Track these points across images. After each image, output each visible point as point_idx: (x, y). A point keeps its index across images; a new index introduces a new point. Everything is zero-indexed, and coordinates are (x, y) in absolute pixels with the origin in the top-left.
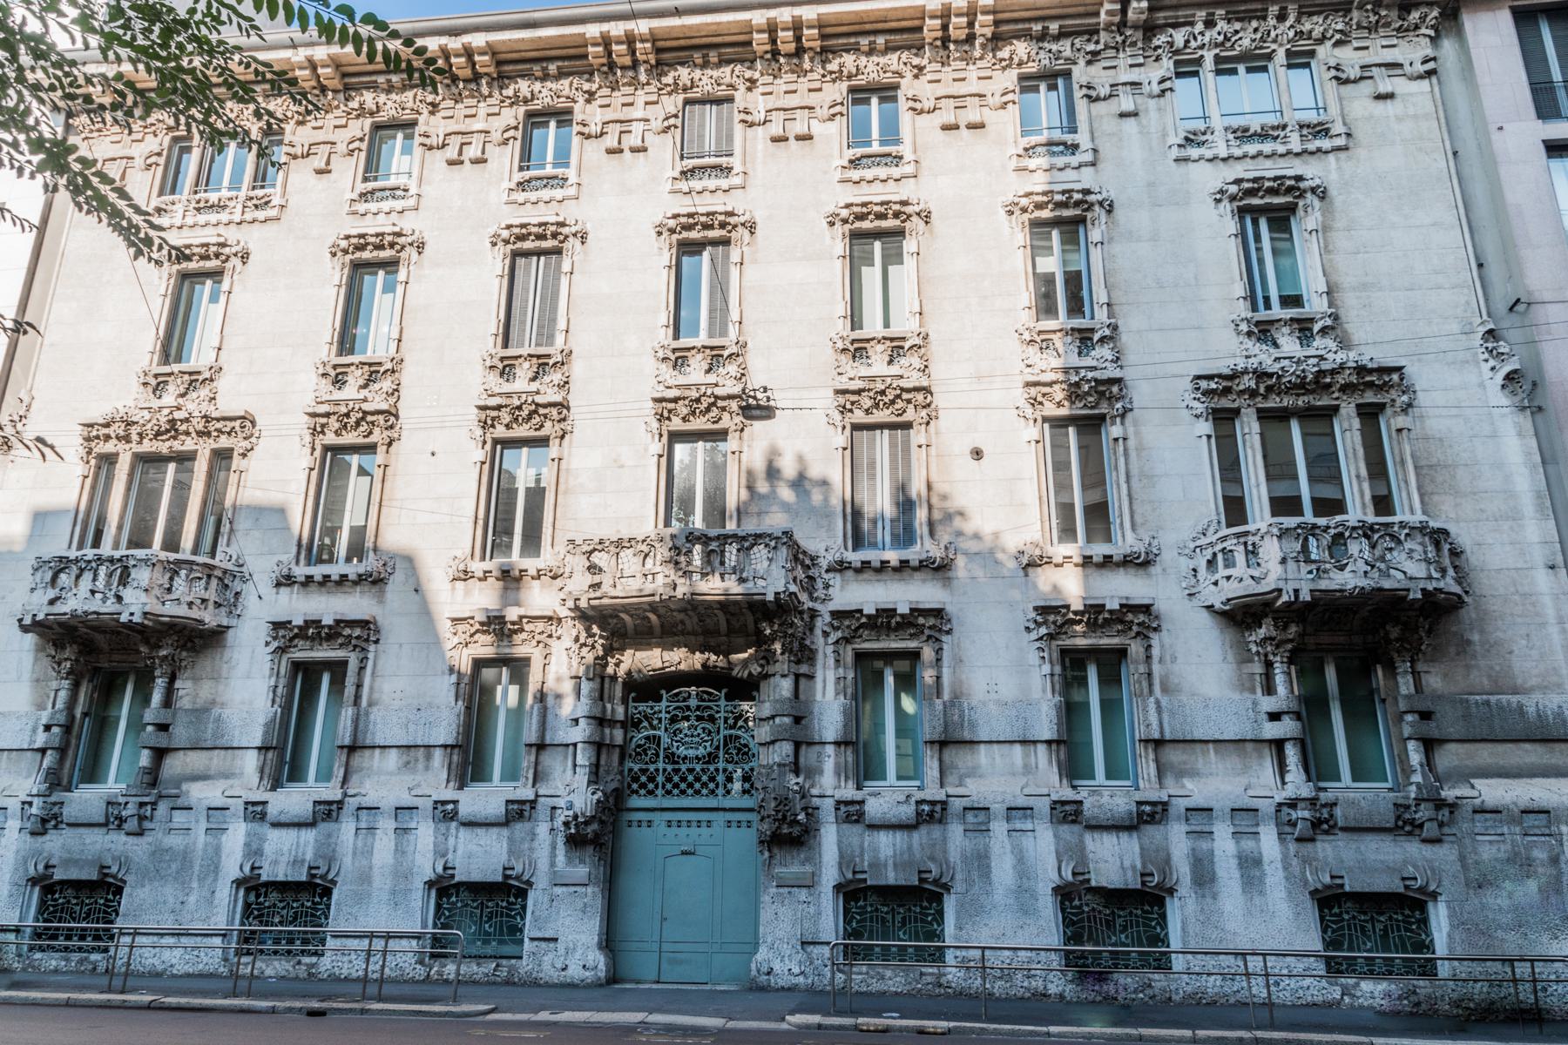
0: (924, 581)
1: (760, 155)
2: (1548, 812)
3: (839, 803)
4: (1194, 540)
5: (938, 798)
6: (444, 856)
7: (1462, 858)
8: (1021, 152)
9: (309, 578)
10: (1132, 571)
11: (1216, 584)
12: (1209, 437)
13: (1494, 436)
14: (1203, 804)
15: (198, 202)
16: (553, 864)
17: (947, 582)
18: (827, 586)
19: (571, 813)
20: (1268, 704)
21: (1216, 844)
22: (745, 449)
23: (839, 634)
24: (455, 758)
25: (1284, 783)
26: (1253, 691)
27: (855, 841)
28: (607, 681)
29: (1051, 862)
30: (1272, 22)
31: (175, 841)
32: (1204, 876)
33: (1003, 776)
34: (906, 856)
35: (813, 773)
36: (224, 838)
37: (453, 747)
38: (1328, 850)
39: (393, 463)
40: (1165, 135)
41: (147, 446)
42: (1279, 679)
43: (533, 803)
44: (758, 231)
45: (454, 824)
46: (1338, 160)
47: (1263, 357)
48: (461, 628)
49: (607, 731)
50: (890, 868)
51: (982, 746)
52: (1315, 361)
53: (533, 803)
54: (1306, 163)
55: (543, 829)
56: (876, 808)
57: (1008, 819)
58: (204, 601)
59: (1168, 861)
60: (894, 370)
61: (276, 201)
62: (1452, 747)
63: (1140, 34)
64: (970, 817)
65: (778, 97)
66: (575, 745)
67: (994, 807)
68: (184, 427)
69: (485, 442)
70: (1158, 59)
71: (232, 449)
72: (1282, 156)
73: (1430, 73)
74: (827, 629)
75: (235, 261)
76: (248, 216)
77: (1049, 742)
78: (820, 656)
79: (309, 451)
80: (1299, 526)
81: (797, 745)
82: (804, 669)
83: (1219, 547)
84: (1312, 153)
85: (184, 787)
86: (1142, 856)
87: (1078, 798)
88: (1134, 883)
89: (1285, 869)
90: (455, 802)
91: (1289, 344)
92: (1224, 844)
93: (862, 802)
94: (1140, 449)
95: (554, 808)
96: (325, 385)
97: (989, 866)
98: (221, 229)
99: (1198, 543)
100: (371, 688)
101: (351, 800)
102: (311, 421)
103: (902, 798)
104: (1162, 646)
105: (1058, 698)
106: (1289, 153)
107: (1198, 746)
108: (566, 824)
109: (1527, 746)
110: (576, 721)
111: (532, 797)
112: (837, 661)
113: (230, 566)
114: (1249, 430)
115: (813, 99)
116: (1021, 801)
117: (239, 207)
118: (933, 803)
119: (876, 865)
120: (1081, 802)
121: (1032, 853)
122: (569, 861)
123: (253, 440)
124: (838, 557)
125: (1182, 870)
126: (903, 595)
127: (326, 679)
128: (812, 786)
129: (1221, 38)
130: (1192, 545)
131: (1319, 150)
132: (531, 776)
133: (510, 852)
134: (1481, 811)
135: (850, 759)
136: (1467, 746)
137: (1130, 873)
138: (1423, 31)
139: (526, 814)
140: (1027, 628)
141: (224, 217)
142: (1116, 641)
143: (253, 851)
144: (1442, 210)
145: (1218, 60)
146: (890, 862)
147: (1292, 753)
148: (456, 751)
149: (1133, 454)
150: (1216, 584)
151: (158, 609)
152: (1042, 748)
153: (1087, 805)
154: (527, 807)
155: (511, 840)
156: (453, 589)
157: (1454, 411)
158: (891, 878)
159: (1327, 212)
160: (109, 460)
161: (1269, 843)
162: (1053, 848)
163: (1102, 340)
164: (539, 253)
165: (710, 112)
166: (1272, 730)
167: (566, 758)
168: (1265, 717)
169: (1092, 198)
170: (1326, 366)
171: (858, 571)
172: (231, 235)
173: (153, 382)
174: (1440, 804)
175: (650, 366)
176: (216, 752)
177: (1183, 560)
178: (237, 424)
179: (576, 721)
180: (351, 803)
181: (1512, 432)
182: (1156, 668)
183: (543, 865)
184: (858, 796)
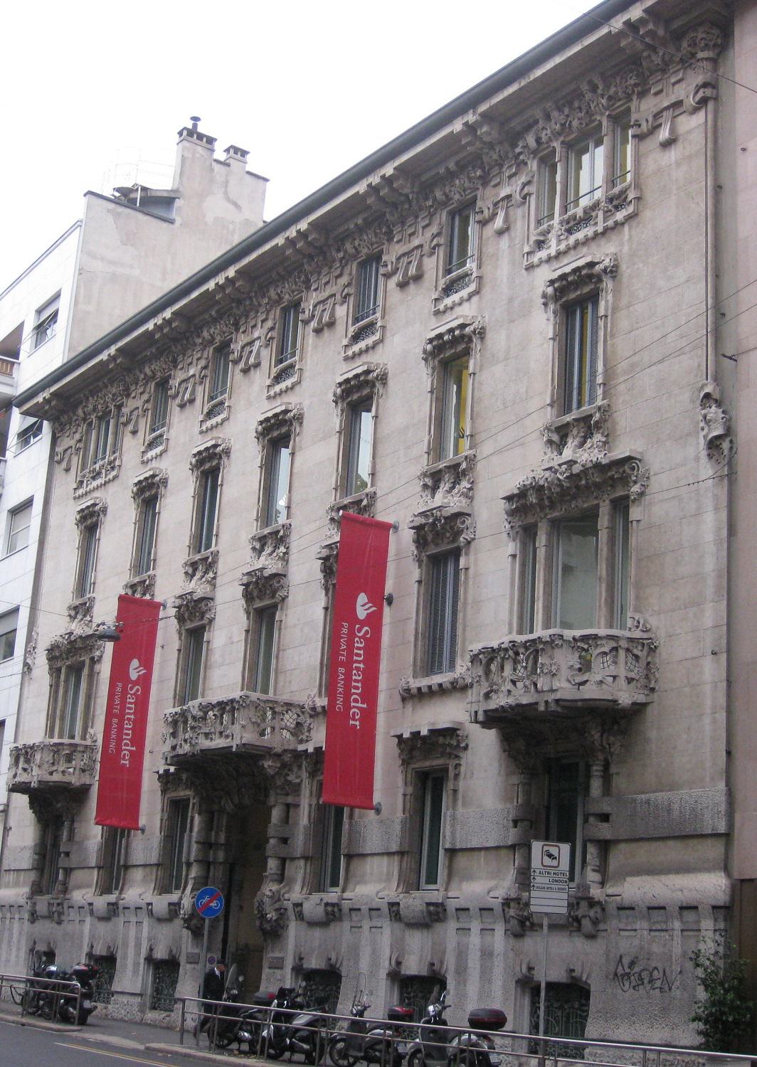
1: (310, 349)
2: (664, 908)
7: (607, 954)
10: (458, 695)
12: (514, 556)
13: (698, 514)
18: (309, 731)
22: (284, 618)
24: (159, 872)
29: (387, 952)
30: (588, 96)
35: (292, 881)
38: (534, 945)
40: (523, 245)
51: (369, 859)
57: (371, 919)
59: (444, 952)
62: (622, 846)
63: (507, 147)
64: (353, 914)
67: (363, 907)
73: (703, 102)
81: (283, 861)
82: (290, 800)
84: (613, 229)
88: (424, 972)
93: (301, 905)
103: (318, 901)
104: (467, 763)
106: (596, 235)
107: (477, 853)
109: (671, 843)
118: (333, 905)
120: (398, 904)
122: (192, 948)
128: (288, 892)
129: (558, 127)
131: (616, 224)
134: (621, 908)
136: (633, 845)
138: (701, 55)
142: (440, 762)
144: (694, 265)
145: (568, 146)
149: (471, 582)
153: (401, 906)
157: (673, 493)
160: (59, 670)
161: (499, 940)
169: (468, 330)
170: (576, 469)
174: (592, 903)
176: (86, 870)
181: (710, 508)
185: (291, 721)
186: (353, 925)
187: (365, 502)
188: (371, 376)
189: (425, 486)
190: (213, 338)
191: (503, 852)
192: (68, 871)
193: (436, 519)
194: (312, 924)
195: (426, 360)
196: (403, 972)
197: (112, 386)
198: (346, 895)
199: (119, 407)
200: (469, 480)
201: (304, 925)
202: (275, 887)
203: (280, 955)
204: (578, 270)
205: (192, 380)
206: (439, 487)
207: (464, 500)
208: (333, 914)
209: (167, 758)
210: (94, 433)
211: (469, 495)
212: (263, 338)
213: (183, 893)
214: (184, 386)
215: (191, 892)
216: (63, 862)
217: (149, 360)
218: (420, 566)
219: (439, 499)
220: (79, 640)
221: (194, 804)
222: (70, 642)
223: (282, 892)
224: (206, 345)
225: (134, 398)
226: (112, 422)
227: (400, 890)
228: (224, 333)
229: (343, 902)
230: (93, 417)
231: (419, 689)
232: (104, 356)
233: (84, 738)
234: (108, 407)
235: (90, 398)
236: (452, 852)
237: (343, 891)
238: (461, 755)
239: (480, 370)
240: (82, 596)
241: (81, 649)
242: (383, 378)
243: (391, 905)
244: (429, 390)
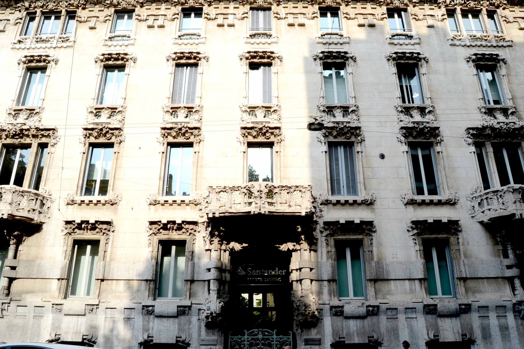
0: (363, 209)
3: (332, 308)
4: (472, 194)
5: (376, 304)
6: (148, 331)
8: (391, 37)
9: (83, 202)
11: (483, 212)
14: (486, 305)
15: (37, 39)
16: (200, 335)
17: (373, 210)
18: (321, 211)
19: (209, 312)
20: (507, 262)
21: (490, 321)
22: (282, 151)
23: (328, 232)
25: (514, 295)
26: (499, 257)
27: (339, 324)
28: (222, 251)
29: (425, 332)
31: (19, 321)
32: (486, 335)
33: (402, 294)
36: (42, 320)
37: (150, 281)
39: (121, 151)
41: (9, 141)
42: (510, 252)
43: (190, 307)
44: (284, 60)
45: (152, 316)
46: (509, 50)
47: (490, 121)
48: (154, 226)
49: (223, 274)
52: (513, 124)
53: (190, 307)
54: (498, 50)
55: (194, 319)
56: (348, 309)
57: (405, 313)
58: (34, 210)
59: (472, 329)
60: (346, 119)
61: (72, 39)
64: (389, 312)
65: (290, 9)
66: (209, 281)
67: (399, 308)
68: (27, 133)
69: (164, 144)
70: (440, 8)
71: (48, 144)
72: (489, 47)
74: (322, 230)
75: (52, 63)
76: (59, 45)
77: (420, 280)
78: (319, 242)
79: (83, 145)
80: (520, 188)
83: (485, 197)
84: (500, 47)
85: (23, 296)
86: (461, 327)
87: (435, 303)
88: (459, 339)
89: (518, 330)
90: (153, 306)
91: (501, 118)
92: (493, 321)
93: (342, 307)
94: (448, 156)
95: (200, 310)
96: (92, 116)
97: (398, 334)
98: (47, 50)
99: (474, 195)
100: (111, 253)
101: (103, 304)
102: (85, 132)
103: (360, 305)
104: (463, 238)
107: (480, 280)
108: (207, 317)
110: (209, 270)
111: (190, 304)
112: (327, 244)
113: (46, 195)
114: (489, 151)
115: (304, 11)
116: (411, 306)
117: (55, 41)
118: (373, 307)
119: (348, 334)
120: (436, 305)
122: (207, 334)
123: (58, 139)
124: (326, 198)
125: (478, 334)
126: (357, 215)
127: (89, 247)
130: (472, 196)
131: (502, 46)
132: (188, 295)
133: (179, 330)
135: (335, 287)
139: (187, 312)
140: (408, 230)
141: (48, 45)
142: (445, 236)
143: (56, 326)
146: (355, 333)
147: (517, 283)
148: (152, 282)
149: (445, 158)
150: (483, 212)
151: (16, 213)
152: (417, 282)
153: (439, 306)
154: (187, 309)
155: (179, 324)
156: (150, 208)
158: (356, 340)
159: (508, 69)
161: (511, 319)
162: (425, 325)
163: (430, 112)
164: (187, 65)
165: (261, 14)
166: (509, 273)
167: (204, 286)
168: (505, 267)
171: (334, 205)
172: (51, 52)
173: (13, 113)
175: (239, 114)
177: (469, 202)
178: (51, 132)
179: (209, 270)
180: (102, 306)
182: (461, 247)
183: (195, 335)
184: (340, 304)
191: (500, 280)
196: (441, 340)
204: (492, 55)
230: (38, 11)
236: (464, 280)
238: (459, 234)
243: (425, 306)
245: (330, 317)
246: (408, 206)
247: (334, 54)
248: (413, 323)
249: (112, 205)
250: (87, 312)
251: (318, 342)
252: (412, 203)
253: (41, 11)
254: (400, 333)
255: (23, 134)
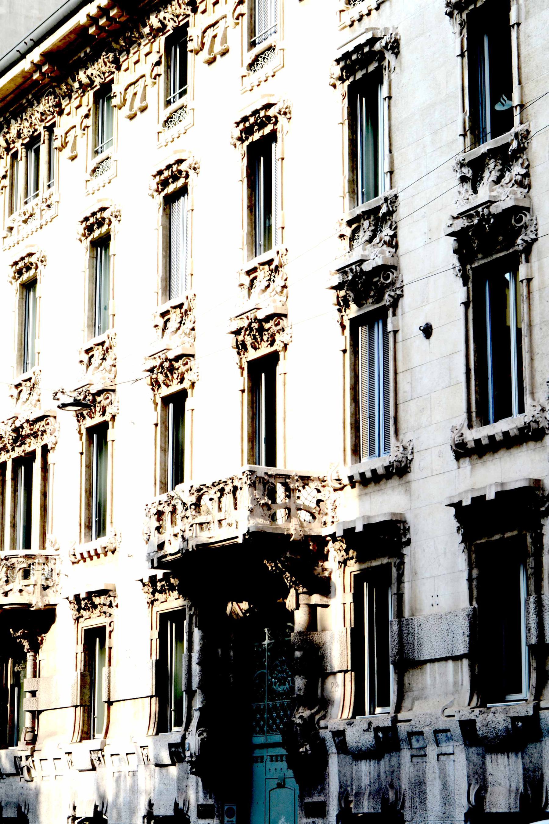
0: (393, 488)
10: (531, 444)
16: (197, 800)
27: (347, 769)
34: (377, 784)
50: (366, 797)
57: (438, 743)
103: (365, 727)
105: (475, 604)
120: (473, 722)
121: (452, 778)
123: (56, 434)
128: (324, 717)
137: (513, 795)
146: (368, 791)
153: (478, 725)
185: (310, 498)
186: (415, 752)
187: (384, 210)
188: (378, 46)
189: (463, 179)
190: (164, 26)
192: (36, 714)
193: (484, 219)
194: (359, 755)
195: (450, 15)
197: (39, 103)
198: (400, 716)
199: (50, 129)
200: (522, 165)
201: (348, 759)
202: (307, 713)
203: (322, 798)
205: (141, 82)
206: (482, 179)
207: (519, 191)
208: (387, 742)
209: (153, 561)
210: (21, 165)
211: (524, 182)
212: (229, 16)
213: (186, 729)
214: (131, 90)
215: (198, 728)
216: (28, 703)
217: (84, 64)
218: (465, 284)
219: (485, 192)
220: (25, 425)
221: (191, 617)
222: (16, 430)
223: (317, 717)
224: (155, 33)
225: (69, 114)
226: (44, 149)
227: (474, 704)
228: (178, 16)
229: (399, 724)
231: (478, 442)
232: (25, 65)
233: (43, 546)
234: (36, 130)
235: (13, 121)
237: (398, 709)
239: (526, 19)
240: (25, 370)
241: (28, 436)
242: (395, 47)
244: (459, 53)
245: (336, 755)
246: (461, 461)
247: (354, 57)
248: (447, 767)
249: (113, 552)
250: (96, 763)
251: (320, 810)
252: (462, 451)
253: (22, 144)
254: (428, 791)
255: (22, 436)
